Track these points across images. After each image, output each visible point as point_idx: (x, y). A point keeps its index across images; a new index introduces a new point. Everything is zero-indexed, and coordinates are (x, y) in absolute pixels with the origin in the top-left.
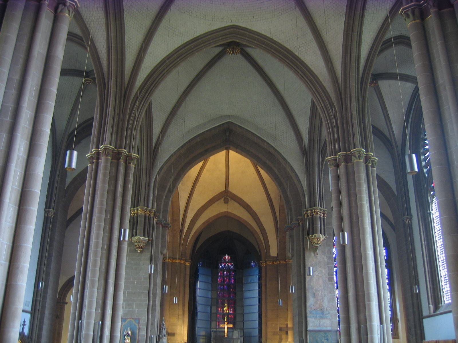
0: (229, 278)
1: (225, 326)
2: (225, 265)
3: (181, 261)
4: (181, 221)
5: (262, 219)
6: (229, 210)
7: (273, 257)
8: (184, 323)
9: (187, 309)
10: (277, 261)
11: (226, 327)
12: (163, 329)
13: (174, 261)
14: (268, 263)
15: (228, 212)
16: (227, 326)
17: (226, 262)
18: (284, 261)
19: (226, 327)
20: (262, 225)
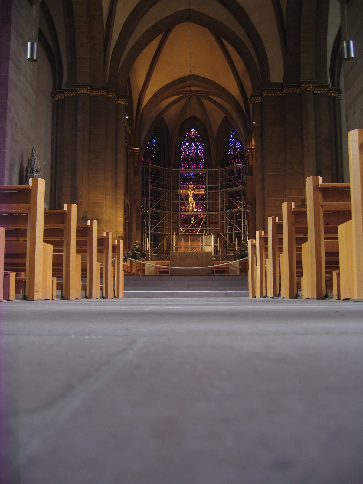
0: (197, 163)
1: (189, 192)
2: (190, 145)
3: (108, 94)
4: (105, 22)
5: (255, 18)
6: (193, 7)
7: (276, 84)
8: (116, 204)
9: (121, 180)
10: (282, 90)
11: (190, 193)
12: (32, 169)
13: (95, 94)
14: (265, 94)
15: (190, 10)
16: (192, 192)
17: (192, 140)
18: (297, 89)
19: (190, 193)
20: (254, 29)
